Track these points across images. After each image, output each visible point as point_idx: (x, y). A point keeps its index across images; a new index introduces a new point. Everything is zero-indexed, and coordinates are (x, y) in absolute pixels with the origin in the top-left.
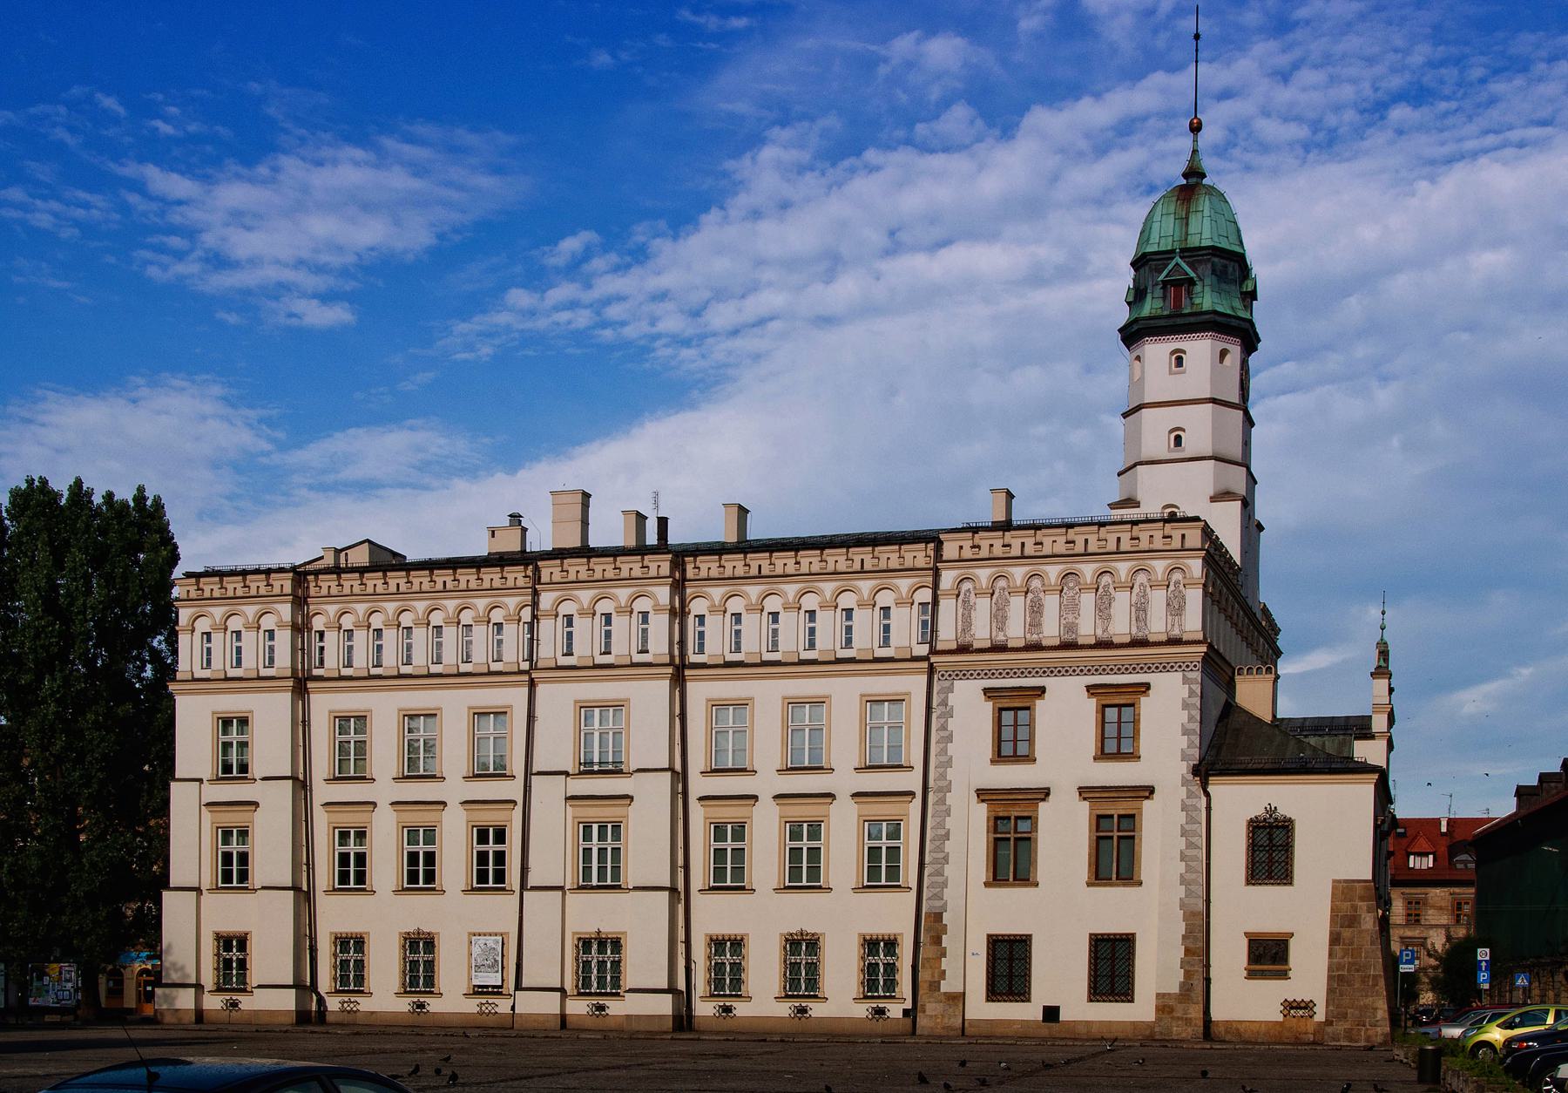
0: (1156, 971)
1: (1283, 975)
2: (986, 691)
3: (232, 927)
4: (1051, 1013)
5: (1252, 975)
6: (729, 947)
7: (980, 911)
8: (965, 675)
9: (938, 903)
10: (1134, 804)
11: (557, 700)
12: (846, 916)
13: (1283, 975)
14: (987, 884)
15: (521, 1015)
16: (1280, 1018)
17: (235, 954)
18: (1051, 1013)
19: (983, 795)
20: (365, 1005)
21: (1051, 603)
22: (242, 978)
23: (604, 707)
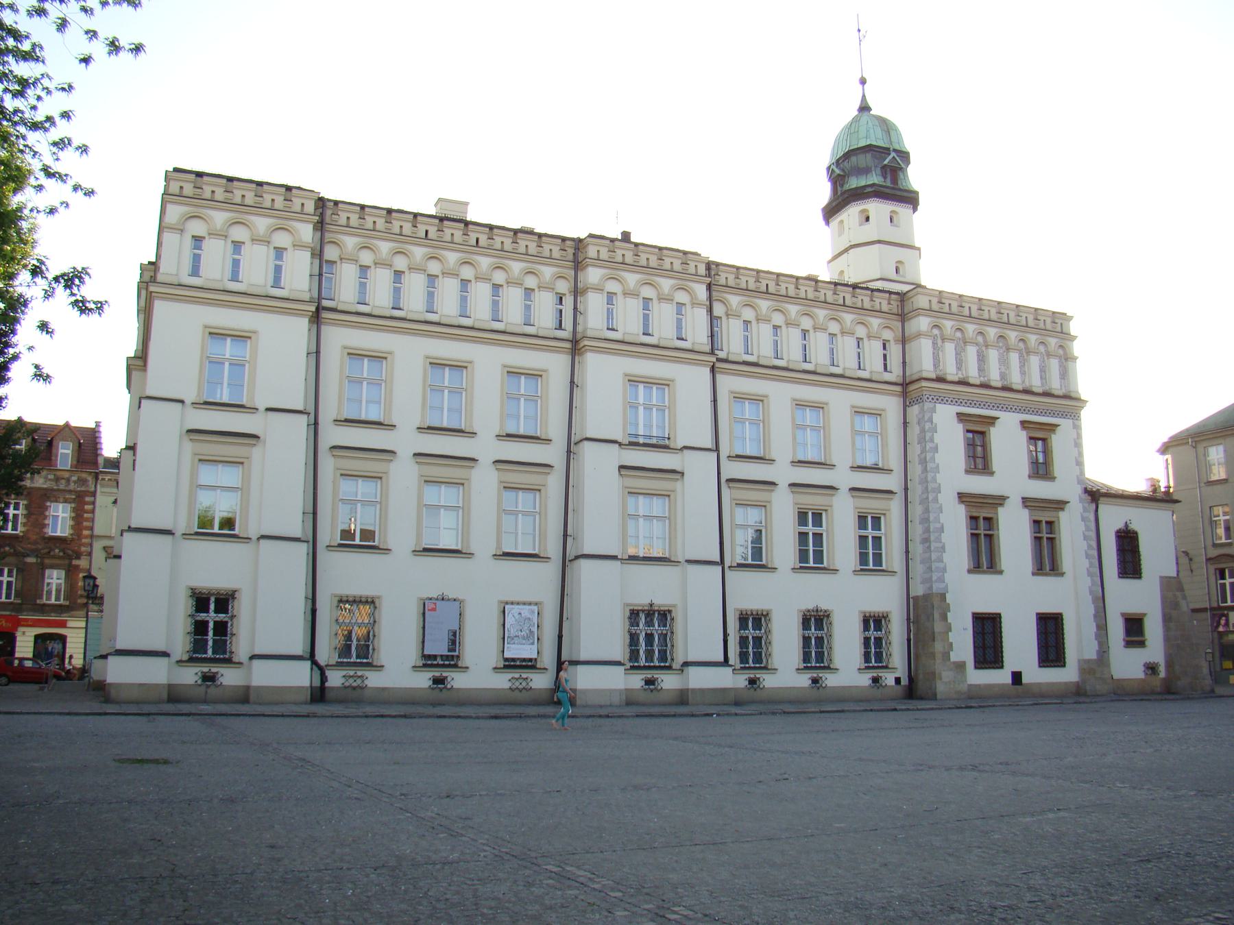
0: (1078, 642)
1: (1142, 644)
2: (958, 414)
3: (213, 581)
4: (1017, 677)
5: (1129, 644)
6: (754, 621)
7: (968, 594)
8: (943, 401)
9: (942, 585)
10: (1053, 514)
11: (604, 374)
12: (850, 596)
13: (1142, 644)
14: (969, 571)
15: (585, 692)
16: (1141, 675)
17: (212, 617)
18: (1017, 677)
19: (962, 497)
20: (374, 680)
21: (993, 355)
22: (221, 646)
23: (649, 382)
